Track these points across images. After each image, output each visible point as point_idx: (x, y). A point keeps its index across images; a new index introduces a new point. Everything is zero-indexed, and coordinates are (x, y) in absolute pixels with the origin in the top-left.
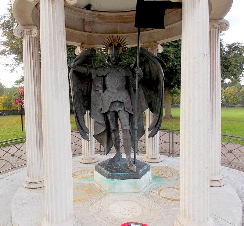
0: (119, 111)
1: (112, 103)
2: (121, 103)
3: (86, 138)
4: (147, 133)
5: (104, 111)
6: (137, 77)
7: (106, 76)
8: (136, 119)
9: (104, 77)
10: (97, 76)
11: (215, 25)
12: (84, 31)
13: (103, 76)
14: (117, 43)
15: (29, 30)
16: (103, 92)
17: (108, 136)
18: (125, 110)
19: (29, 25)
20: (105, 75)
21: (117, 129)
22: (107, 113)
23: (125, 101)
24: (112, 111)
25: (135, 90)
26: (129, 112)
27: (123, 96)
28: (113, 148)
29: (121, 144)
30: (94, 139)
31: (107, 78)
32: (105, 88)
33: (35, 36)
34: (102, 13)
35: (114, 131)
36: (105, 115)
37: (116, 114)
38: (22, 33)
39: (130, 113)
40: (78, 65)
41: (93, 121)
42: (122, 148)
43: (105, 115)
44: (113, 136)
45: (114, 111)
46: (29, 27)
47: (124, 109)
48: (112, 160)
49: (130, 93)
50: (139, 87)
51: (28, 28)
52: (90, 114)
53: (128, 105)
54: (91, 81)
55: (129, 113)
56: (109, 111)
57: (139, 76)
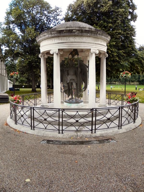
1: (71, 79)
2: (74, 80)
7: (68, 70)
8: (78, 85)
9: (68, 71)
19: (43, 54)
20: (68, 70)
21: (72, 88)
23: (75, 79)
24: (70, 82)
27: (74, 77)
35: (71, 89)
36: (68, 84)
37: (72, 83)
43: (68, 84)
44: (71, 91)
45: (71, 82)
48: (70, 99)
49: (76, 76)
50: (79, 74)
53: (76, 80)
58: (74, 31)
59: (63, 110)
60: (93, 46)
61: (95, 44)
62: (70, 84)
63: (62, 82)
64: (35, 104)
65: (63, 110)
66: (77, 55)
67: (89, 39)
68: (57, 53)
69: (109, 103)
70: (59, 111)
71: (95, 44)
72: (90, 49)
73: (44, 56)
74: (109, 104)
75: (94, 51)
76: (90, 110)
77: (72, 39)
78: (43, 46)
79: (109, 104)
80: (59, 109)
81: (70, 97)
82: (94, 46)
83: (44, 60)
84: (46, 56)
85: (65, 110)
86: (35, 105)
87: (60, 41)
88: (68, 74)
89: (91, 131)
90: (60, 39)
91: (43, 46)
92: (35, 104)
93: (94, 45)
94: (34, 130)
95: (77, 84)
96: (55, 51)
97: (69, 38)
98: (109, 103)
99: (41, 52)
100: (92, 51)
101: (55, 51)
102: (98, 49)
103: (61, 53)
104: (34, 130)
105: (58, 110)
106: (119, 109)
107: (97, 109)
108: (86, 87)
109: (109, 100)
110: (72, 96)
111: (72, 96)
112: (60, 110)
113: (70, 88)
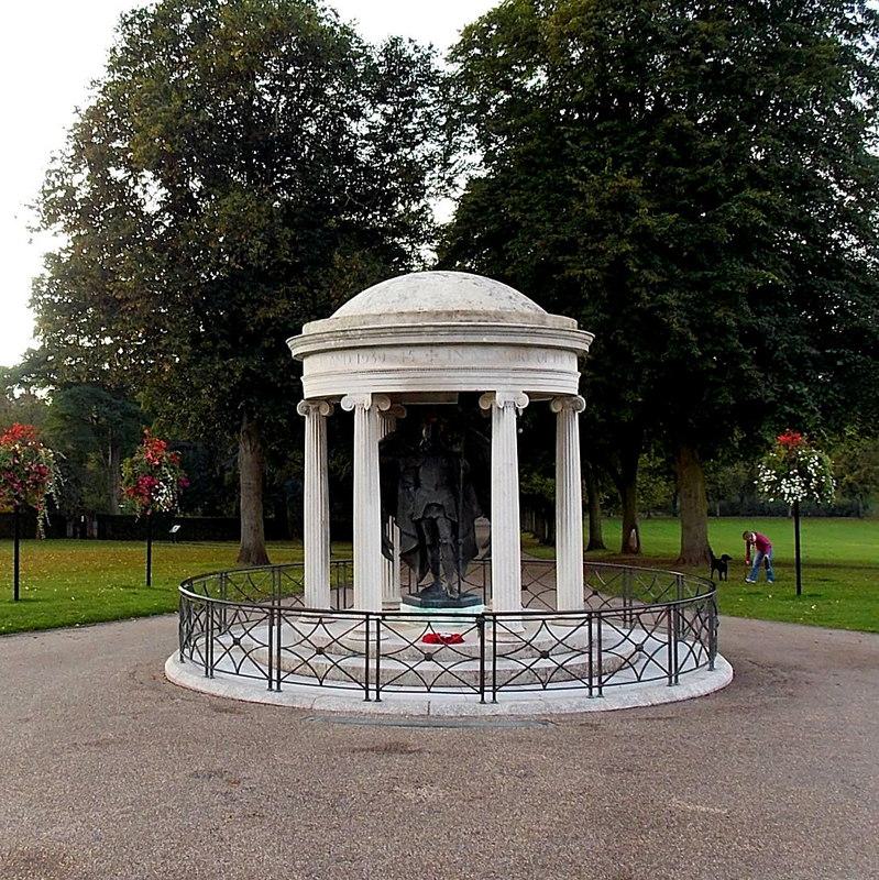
2: (440, 507)
16: (415, 490)
23: (446, 504)
32: (417, 485)
33: (326, 414)
37: (433, 522)
42: (442, 572)
43: (417, 524)
45: (431, 518)
59: (380, 617)
60: (505, 381)
65: (380, 617)
70: (367, 620)
76: (474, 619)
78: (315, 376)
80: (368, 614)
81: (429, 579)
83: (319, 426)
84: (326, 411)
85: (387, 617)
89: (480, 696)
91: (315, 376)
94: (279, 690)
95: (454, 528)
99: (305, 397)
100: (499, 399)
103: (386, 407)
104: (279, 690)
105: (364, 617)
106: (589, 619)
107: (498, 618)
110: (436, 574)
111: (436, 574)
112: (371, 617)
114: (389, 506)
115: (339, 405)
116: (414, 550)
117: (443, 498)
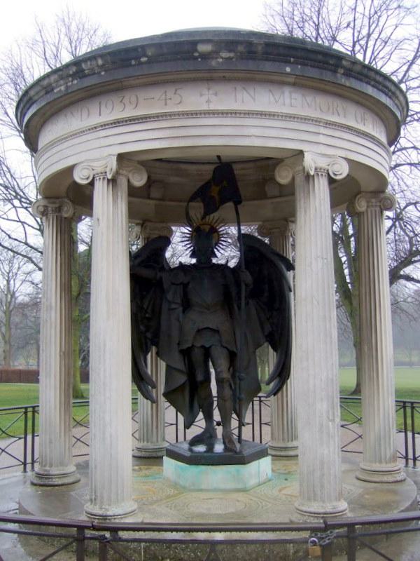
0: (210, 347)
1: (199, 331)
2: (216, 331)
3: (147, 396)
4: (266, 389)
5: (185, 346)
6: (243, 287)
7: (188, 283)
9: (185, 286)
10: (173, 284)
11: (373, 200)
12: (149, 198)
13: (181, 283)
14: (209, 227)
15: (57, 205)
16: (184, 312)
17: (189, 394)
18: (222, 346)
19: (58, 198)
20: (185, 282)
22: (189, 348)
24: (199, 345)
25: (239, 308)
26: (229, 347)
28: (201, 415)
29: (215, 404)
30: (162, 399)
31: (190, 286)
32: (187, 305)
33: (66, 216)
34: (183, 166)
37: (207, 353)
38: (45, 210)
39: (231, 349)
40: (139, 265)
41: (163, 365)
42: (217, 416)
43: (186, 353)
45: (203, 347)
46: (57, 201)
47: (221, 342)
48: (196, 441)
49: (231, 314)
50: (247, 304)
51: (54, 203)
52: (158, 354)
54: (163, 291)
55: (228, 350)
56: (193, 346)
57: (246, 285)
58: (203, 48)
61: (329, 124)
62: (197, 355)
63: (157, 346)
64: (29, 460)
66: (230, 205)
67: (294, 95)
68: (110, 177)
69: (411, 455)
71: (329, 124)
72: (301, 153)
73: (59, 209)
74: (406, 458)
75: (322, 163)
77: (195, 98)
79: (406, 458)
81: (200, 424)
82: (322, 139)
86: (25, 464)
87: (129, 113)
88: (187, 305)
90: (126, 101)
92: (29, 460)
93: (322, 130)
96: (99, 167)
97: (179, 92)
98: (411, 455)
100: (310, 161)
101: (99, 170)
102: (343, 154)
108: (283, 372)
109: (410, 435)
110: (208, 417)
111: (208, 417)
113: (200, 377)
114: (146, 332)
115: (75, 183)
116: (182, 388)
117: (216, 320)
